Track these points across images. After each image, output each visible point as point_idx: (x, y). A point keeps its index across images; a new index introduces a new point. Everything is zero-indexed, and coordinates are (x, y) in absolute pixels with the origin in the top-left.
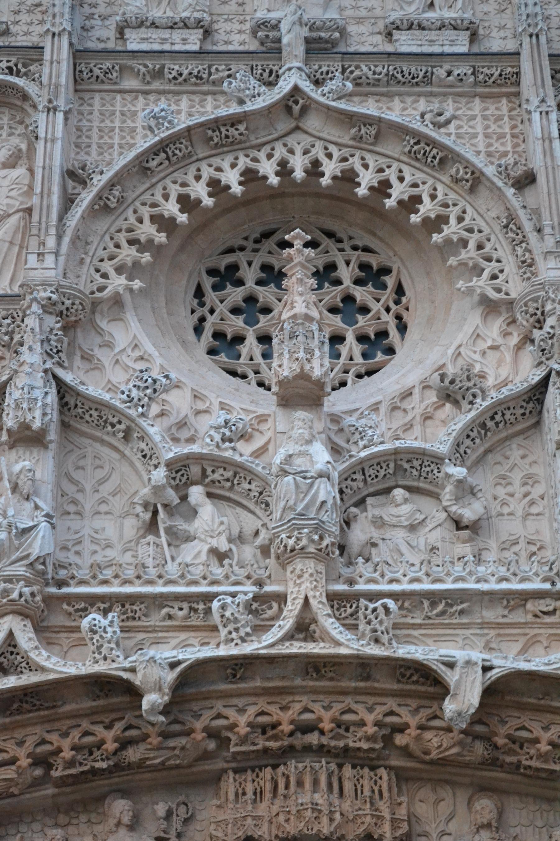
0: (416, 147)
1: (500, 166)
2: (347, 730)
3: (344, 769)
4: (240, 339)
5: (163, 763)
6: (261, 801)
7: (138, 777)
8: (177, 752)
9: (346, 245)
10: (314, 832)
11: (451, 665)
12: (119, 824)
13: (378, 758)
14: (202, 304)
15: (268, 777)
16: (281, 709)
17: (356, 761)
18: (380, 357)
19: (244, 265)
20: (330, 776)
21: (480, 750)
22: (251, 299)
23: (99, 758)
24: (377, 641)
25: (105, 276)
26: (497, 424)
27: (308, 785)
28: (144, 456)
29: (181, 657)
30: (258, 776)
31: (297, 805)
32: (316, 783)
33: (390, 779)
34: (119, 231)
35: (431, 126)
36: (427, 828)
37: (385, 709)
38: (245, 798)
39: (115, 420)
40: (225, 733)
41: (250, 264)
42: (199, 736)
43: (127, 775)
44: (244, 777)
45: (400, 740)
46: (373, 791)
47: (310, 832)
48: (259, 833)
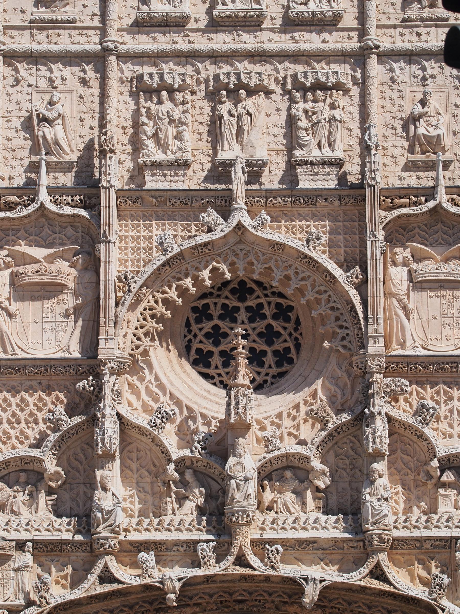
0: (305, 260)
1: (348, 277)
4: (210, 354)
9: (268, 292)
11: (306, 580)
14: (190, 331)
18: (286, 367)
19: (212, 307)
22: (216, 328)
24: (273, 567)
25: (139, 339)
26: (339, 433)
28: (163, 453)
29: (183, 576)
34: (145, 309)
35: (312, 249)
39: (148, 433)
41: (215, 304)
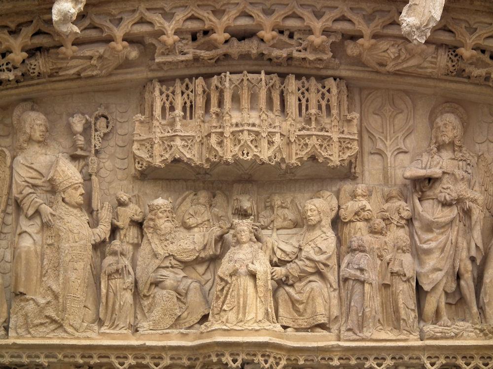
2: (291, 36)
3: (286, 81)
5: (78, 74)
6: (191, 118)
7: (49, 86)
8: (94, 62)
10: (249, 158)
12: (30, 140)
13: (326, 68)
15: (200, 90)
16: (214, 12)
17: (302, 71)
20: (269, 91)
21: (443, 59)
23: (4, 67)
27: (245, 103)
30: (187, 87)
31: (232, 125)
32: (254, 98)
33: (339, 93)
36: (380, 145)
37: (336, 14)
38: (173, 114)
40: (149, 40)
42: (119, 45)
43: (38, 84)
44: (171, 89)
45: (352, 49)
46: (320, 107)
47: (245, 158)
48: (188, 156)
